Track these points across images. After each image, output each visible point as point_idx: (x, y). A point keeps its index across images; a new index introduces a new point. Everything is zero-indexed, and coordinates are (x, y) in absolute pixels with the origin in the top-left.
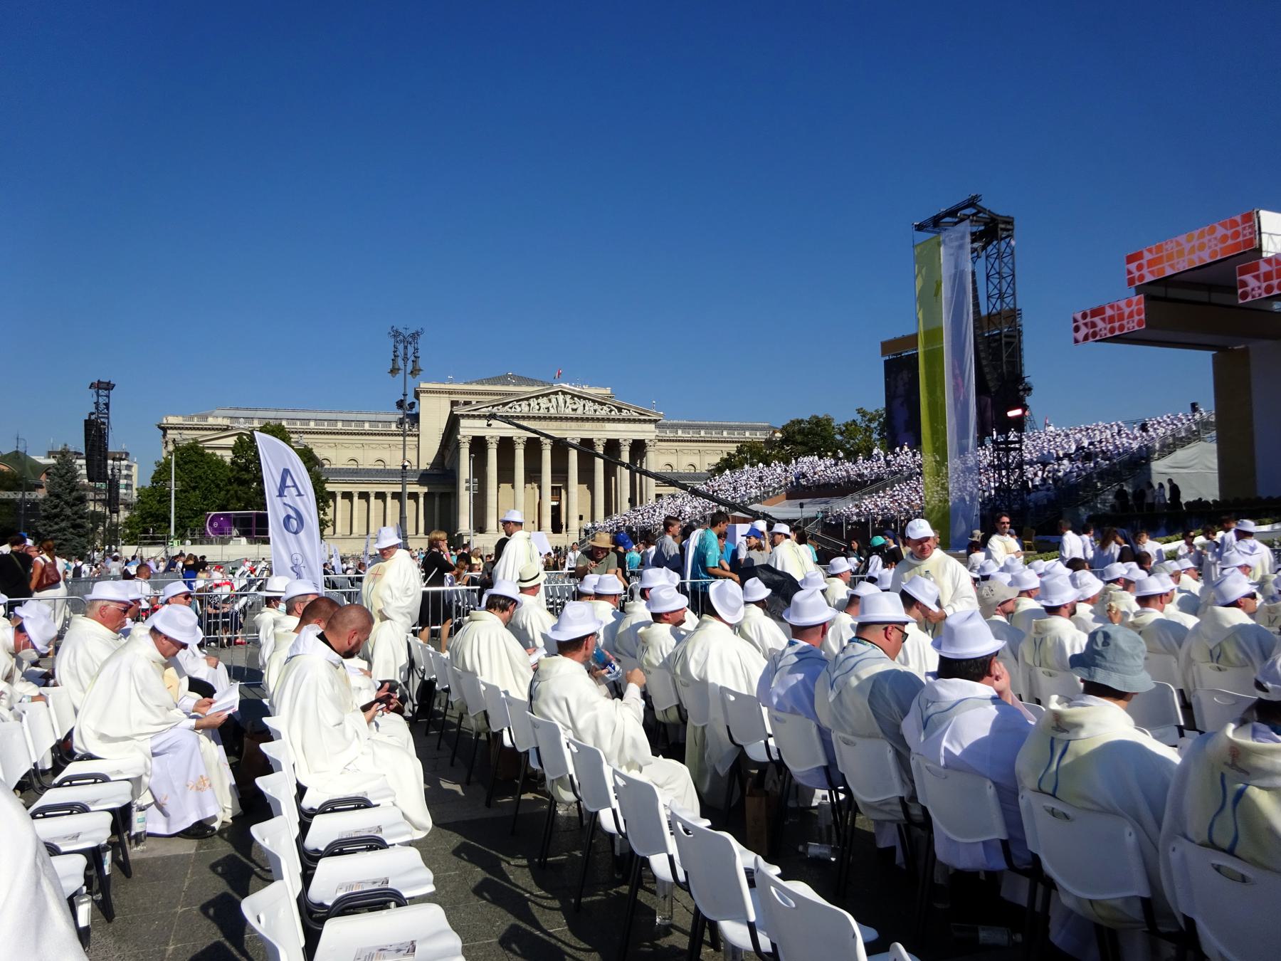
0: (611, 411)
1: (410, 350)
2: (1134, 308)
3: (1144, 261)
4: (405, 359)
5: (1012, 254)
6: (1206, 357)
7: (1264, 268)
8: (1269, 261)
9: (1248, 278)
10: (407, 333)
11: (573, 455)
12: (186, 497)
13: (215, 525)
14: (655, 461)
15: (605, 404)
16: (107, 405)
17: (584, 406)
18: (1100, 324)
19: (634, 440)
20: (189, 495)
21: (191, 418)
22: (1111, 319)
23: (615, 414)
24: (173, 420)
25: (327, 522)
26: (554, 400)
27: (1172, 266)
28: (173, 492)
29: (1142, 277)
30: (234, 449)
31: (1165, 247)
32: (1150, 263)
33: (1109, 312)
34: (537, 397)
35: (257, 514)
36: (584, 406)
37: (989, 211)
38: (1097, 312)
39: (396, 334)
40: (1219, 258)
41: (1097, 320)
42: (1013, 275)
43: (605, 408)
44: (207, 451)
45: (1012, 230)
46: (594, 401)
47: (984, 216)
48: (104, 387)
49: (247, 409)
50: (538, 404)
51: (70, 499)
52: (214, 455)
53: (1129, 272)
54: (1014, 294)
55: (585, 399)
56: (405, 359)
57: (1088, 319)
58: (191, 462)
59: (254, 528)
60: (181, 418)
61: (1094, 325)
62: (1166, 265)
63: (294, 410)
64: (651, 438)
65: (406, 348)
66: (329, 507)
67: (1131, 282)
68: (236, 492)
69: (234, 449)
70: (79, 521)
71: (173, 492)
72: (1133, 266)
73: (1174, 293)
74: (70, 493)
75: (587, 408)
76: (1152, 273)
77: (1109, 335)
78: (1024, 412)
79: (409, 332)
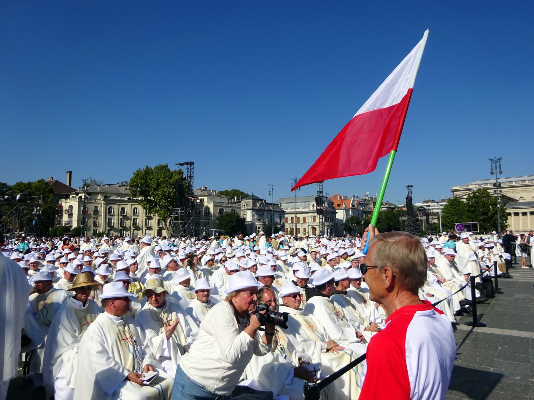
1: (498, 164)
4: (496, 168)
10: (495, 159)
12: (453, 218)
13: (458, 228)
16: (411, 192)
20: (454, 217)
21: (463, 186)
24: (455, 188)
25: (507, 225)
28: (440, 217)
30: (467, 199)
35: (472, 224)
39: (492, 160)
44: (461, 200)
48: (408, 187)
49: (485, 180)
51: (413, 220)
52: (463, 201)
56: (496, 168)
58: (455, 205)
59: (472, 229)
60: (459, 187)
63: (506, 178)
65: (496, 164)
66: (508, 219)
68: (468, 215)
69: (467, 199)
70: (417, 227)
71: (440, 217)
74: (414, 218)
79: (496, 159)
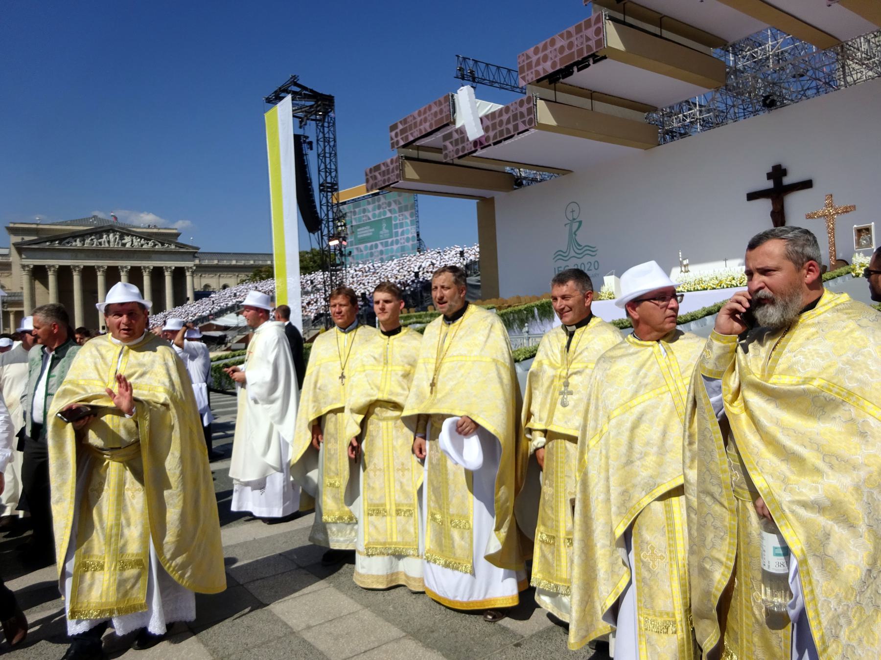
0: (155, 245)
2: (394, 165)
3: (398, 130)
5: (334, 123)
6: (474, 203)
7: (456, 136)
8: (457, 131)
9: (447, 143)
11: (76, 278)
14: (192, 284)
15: (150, 240)
17: (132, 241)
18: (379, 177)
19: (176, 267)
22: (383, 174)
23: (159, 247)
26: (105, 236)
27: (412, 134)
29: (398, 142)
31: (408, 120)
32: (403, 131)
33: (383, 168)
34: (91, 234)
36: (132, 241)
37: (311, 91)
38: (377, 168)
40: (434, 128)
41: (377, 174)
42: (335, 142)
43: (151, 243)
45: (333, 105)
46: (141, 238)
47: (307, 92)
50: (92, 240)
53: (392, 139)
54: (335, 154)
55: (133, 236)
57: (374, 174)
61: (375, 178)
62: (409, 133)
64: (190, 266)
67: (393, 146)
72: (393, 134)
73: (423, 155)
75: (135, 244)
76: (402, 139)
77: (383, 185)
78: (341, 242)
